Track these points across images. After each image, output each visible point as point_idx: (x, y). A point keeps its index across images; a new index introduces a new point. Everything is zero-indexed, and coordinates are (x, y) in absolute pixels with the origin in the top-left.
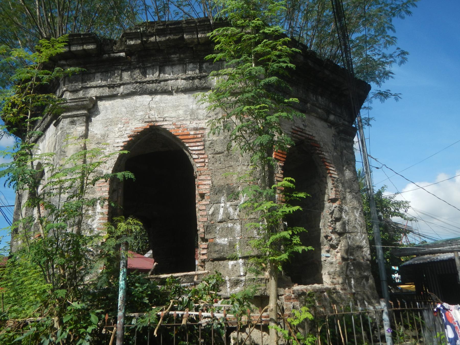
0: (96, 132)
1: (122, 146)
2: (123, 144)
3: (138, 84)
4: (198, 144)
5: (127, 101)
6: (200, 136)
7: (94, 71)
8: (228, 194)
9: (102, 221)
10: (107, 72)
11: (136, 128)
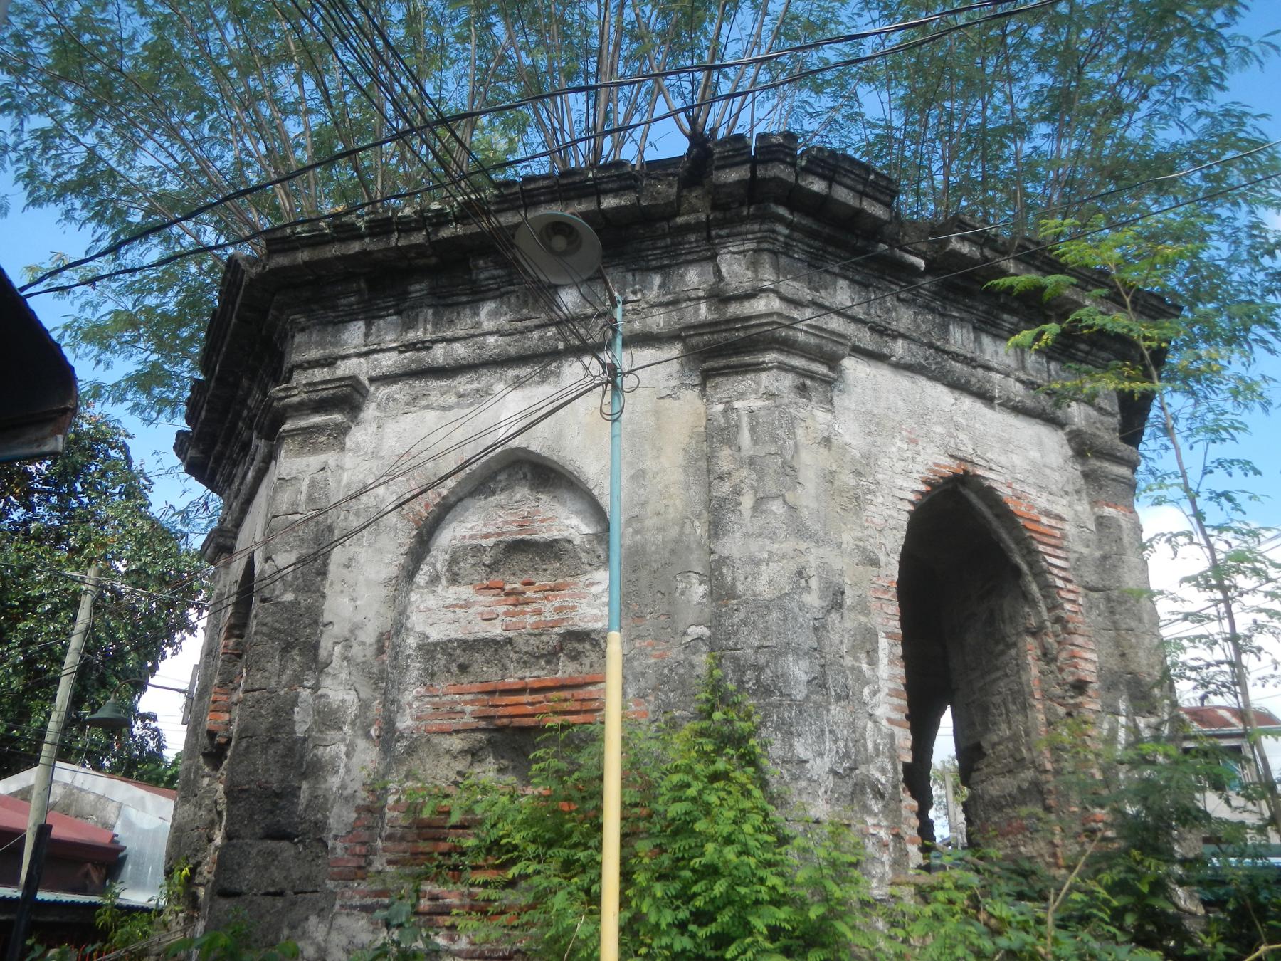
0: (847, 439)
1: (910, 502)
2: (912, 497)
3: (932, 351)
4: (1059, 552)
5: (904, 382)
6: (1058, 533)
7: (837, 270)
8: (1132, 698)
9: (895, 701)
10: (865, 286)
11: (936, 465)
